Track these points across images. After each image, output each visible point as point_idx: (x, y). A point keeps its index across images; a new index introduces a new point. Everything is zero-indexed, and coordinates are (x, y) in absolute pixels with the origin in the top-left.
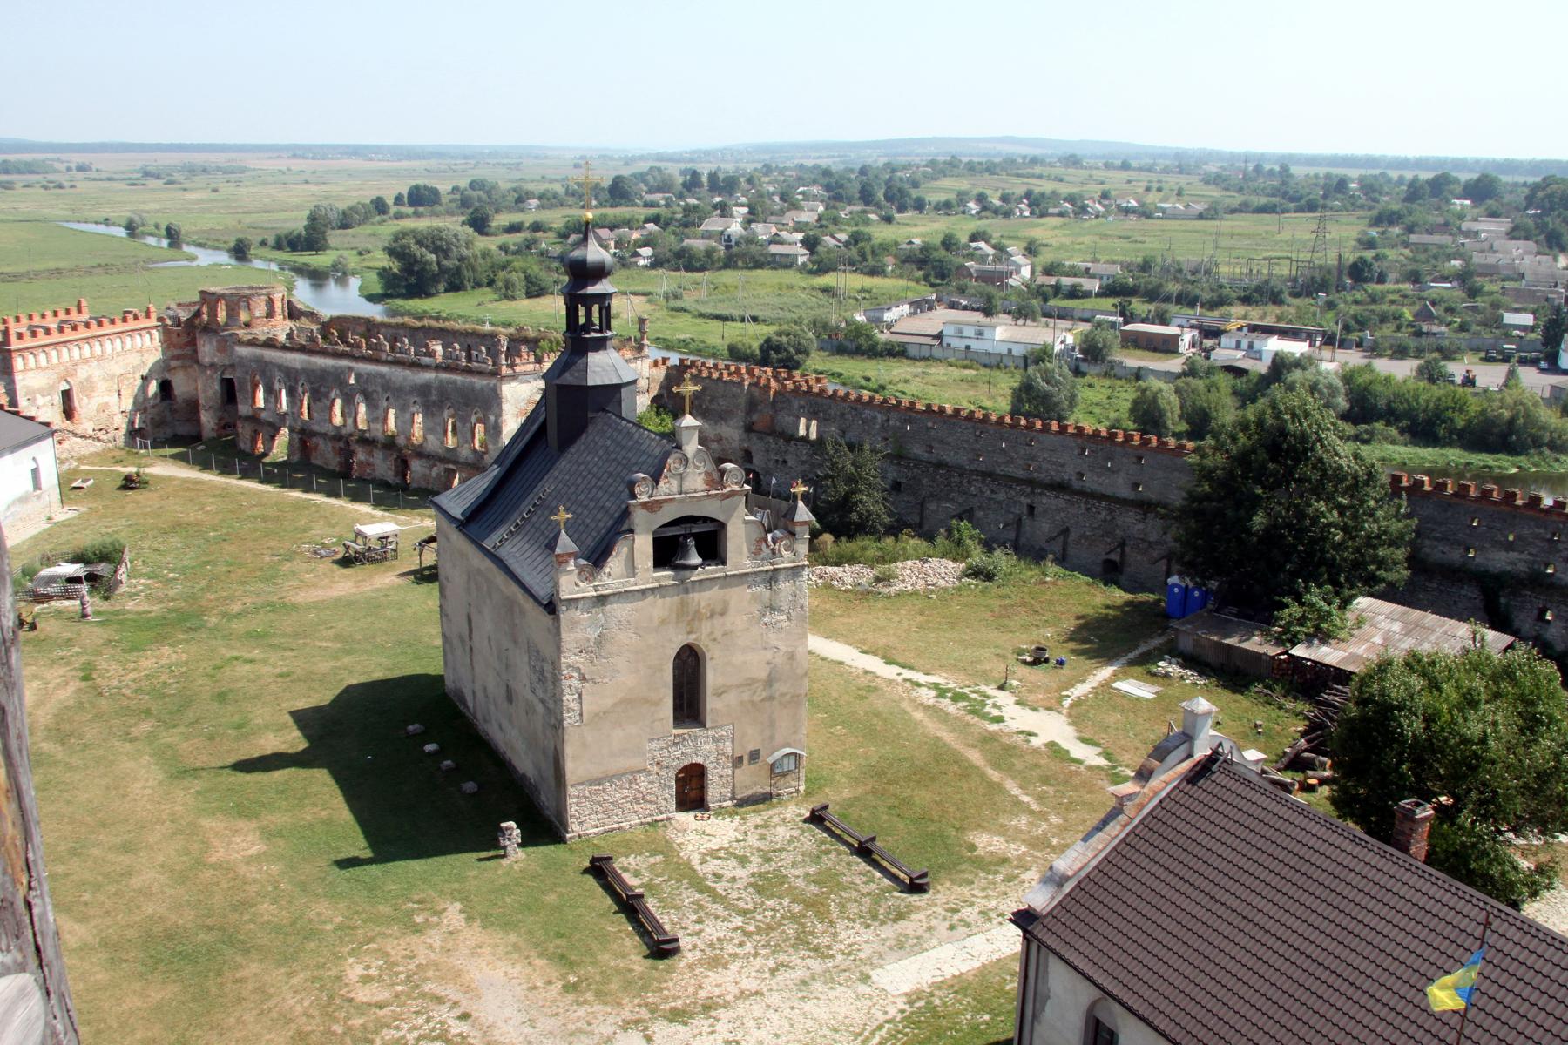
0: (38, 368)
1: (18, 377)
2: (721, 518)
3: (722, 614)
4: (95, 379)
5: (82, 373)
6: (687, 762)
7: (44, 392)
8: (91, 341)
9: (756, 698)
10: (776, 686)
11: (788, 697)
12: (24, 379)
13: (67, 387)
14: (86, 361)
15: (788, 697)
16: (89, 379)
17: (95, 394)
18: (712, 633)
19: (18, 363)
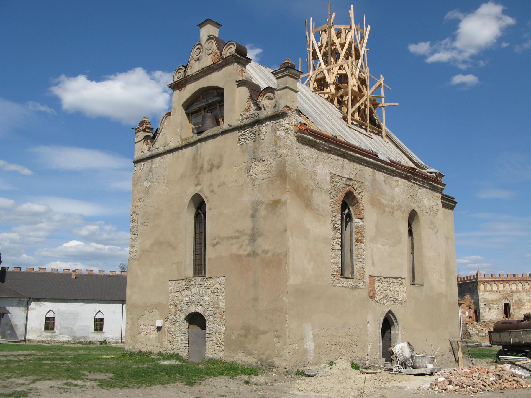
0: (492, 291)
1: (480, 294)
2: (221, 86)
3: (218, 167)
4: (524, 301)
5: (515, 297)
6: (193, 309)
7: (492, 301)
8: (522, 282)
9: (241, 252)
10: (260, 240)
11: (270, 254)
12: (483, 295)
13: (508, 302)
14: (519, 291)
15: (270, 254)
16: (520, 300)
17: (523, 308)
18: (211, 185)
19: (481, 287)
